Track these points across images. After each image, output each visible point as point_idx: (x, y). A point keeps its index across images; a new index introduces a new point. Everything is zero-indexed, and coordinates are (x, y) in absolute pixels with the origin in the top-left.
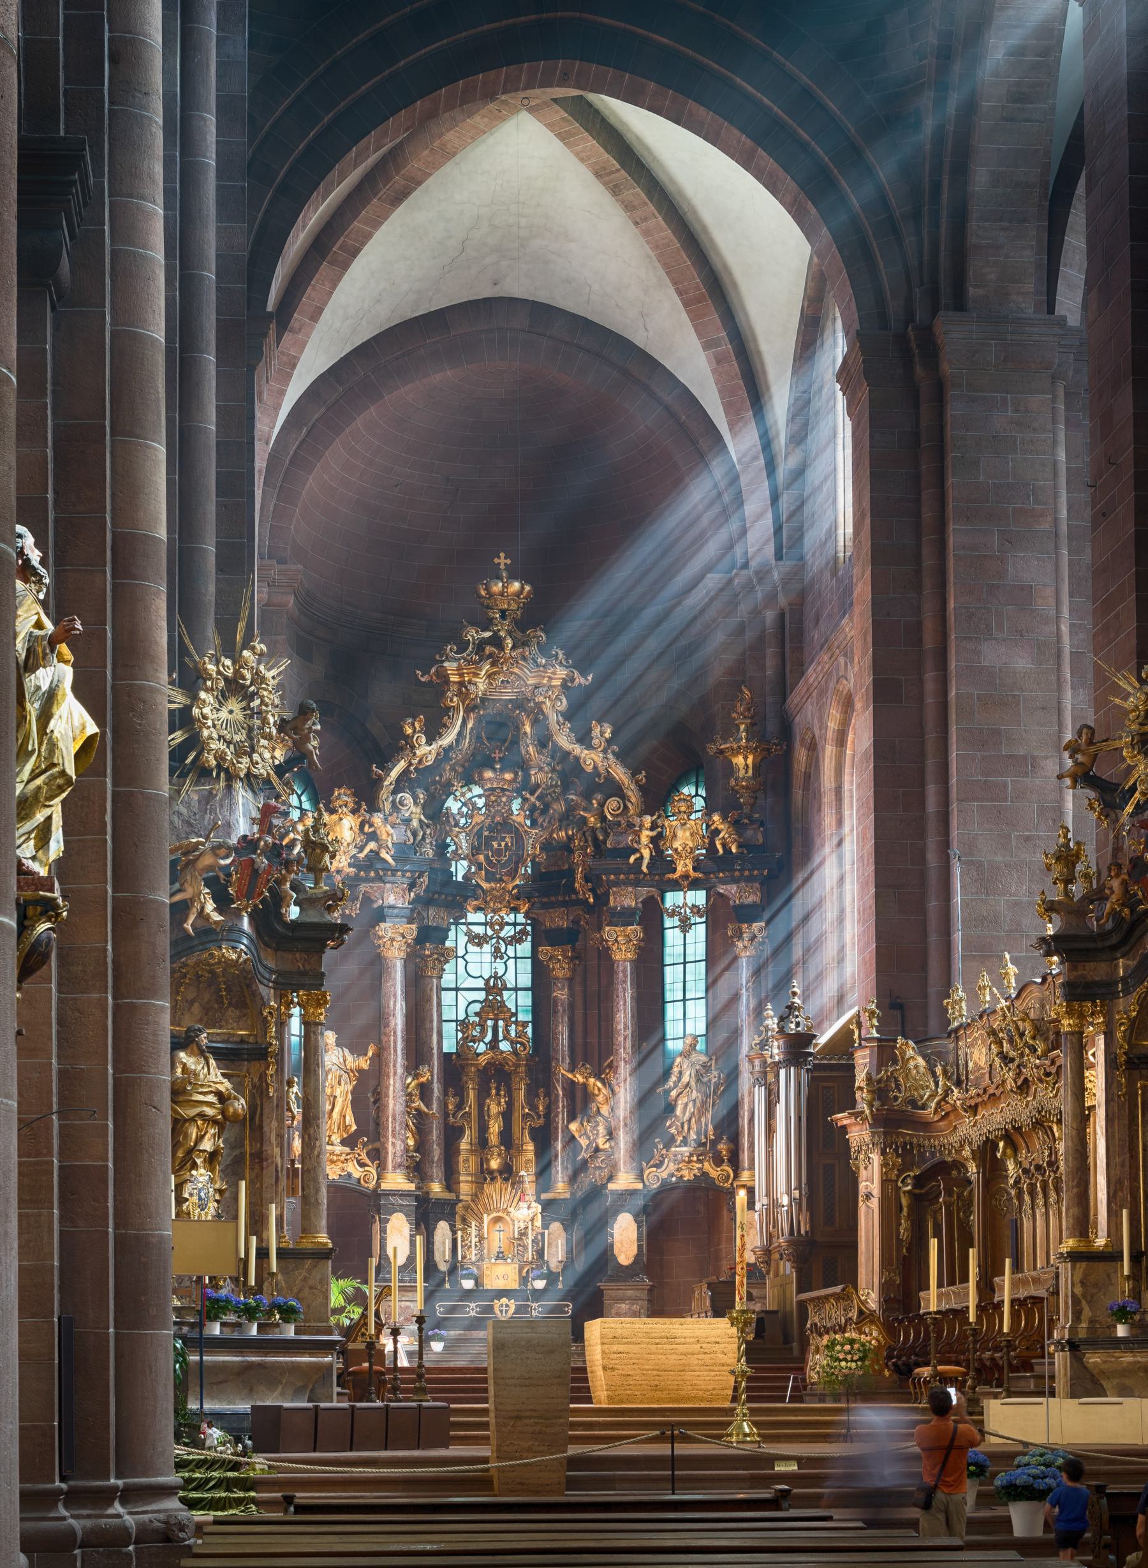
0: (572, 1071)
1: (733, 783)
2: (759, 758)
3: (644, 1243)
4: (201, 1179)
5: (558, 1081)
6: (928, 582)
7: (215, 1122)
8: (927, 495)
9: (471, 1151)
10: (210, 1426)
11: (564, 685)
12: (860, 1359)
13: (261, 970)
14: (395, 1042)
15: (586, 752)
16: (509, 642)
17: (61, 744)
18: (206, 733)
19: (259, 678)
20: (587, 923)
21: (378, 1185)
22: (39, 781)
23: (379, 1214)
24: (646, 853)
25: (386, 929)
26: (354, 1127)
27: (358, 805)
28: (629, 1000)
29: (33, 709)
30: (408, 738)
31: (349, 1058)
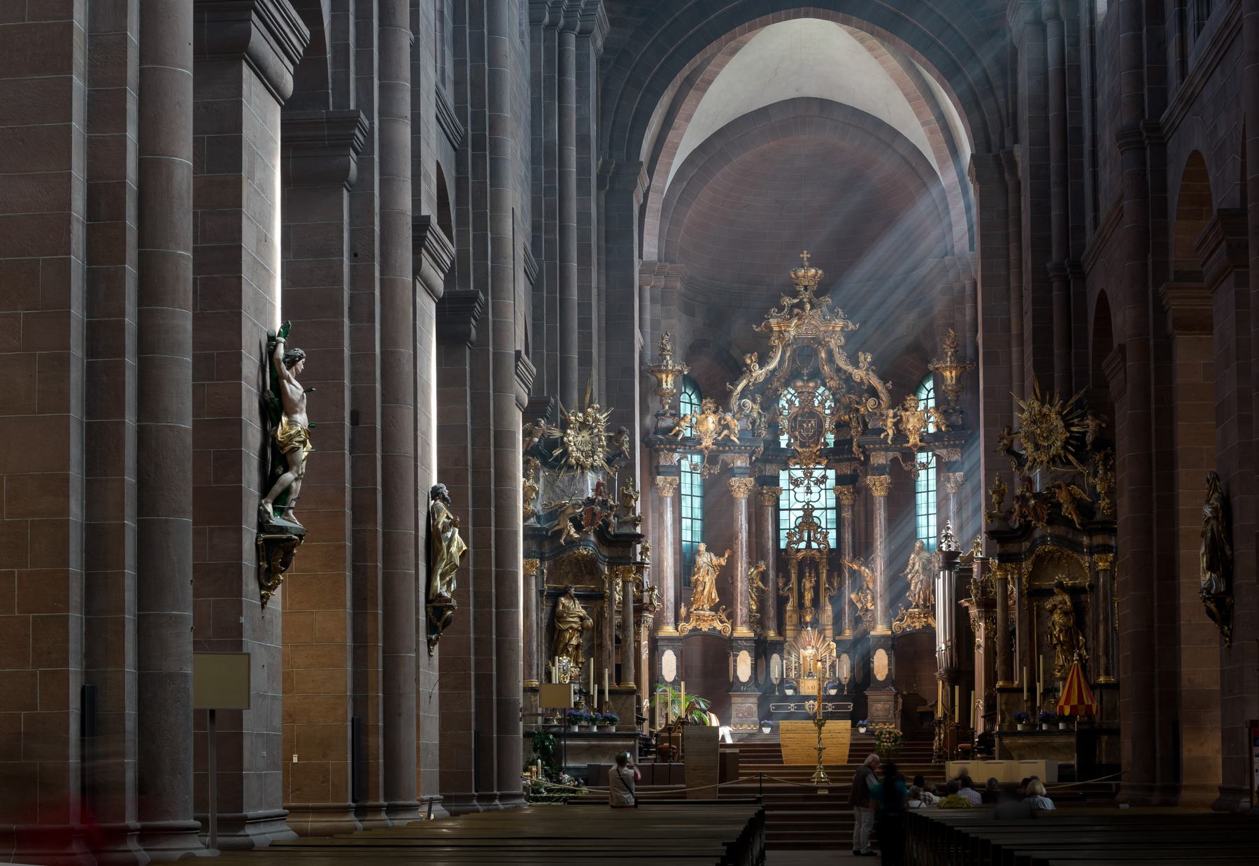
0: (851, 563)
1: (943, 388)
2: (959, 373)
3: (893, 667)
4: (564, 661)
5: (845, 568)
6: (1013, 296)
7: (578, 631)
8: (1013, 246)
9: (793, 611)
10: (564, 774)
11: (842, 328)
12: (893, 741)
13: (601, 557)
14: (742, 549)
15: (856, 371)
16: (808, 306)
17: (454, 555)
18: (570, 448)
19: (596, 420)
20: (861, 472)
21: (732, 633)
22: (447, 567)
23: (733, 651)
24: (891, 432)
26: (718, 600)
27: (717, 408)
28: (883, 520)
29: (445, 544)
30: (747, 366)
31: (714, 559)
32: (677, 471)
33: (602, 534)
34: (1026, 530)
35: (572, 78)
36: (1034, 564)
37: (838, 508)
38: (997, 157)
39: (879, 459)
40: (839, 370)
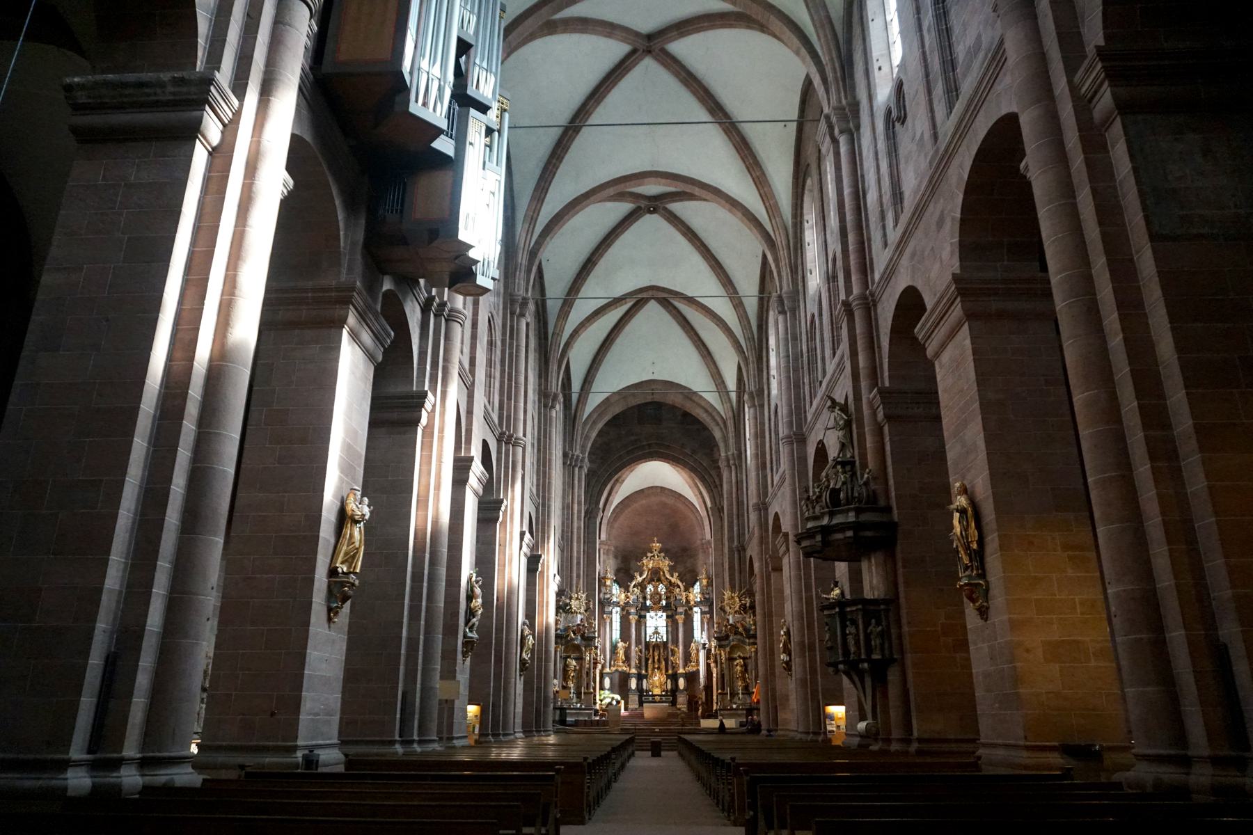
25: (631, 617)
32: (611, 613)
33: (583, 636)
34: (727, 637)
35: (576, 482)
36: (731, 648)
37: (667, 626)
38: (718, 509)
39: (680, 610)
40: (667, 578)
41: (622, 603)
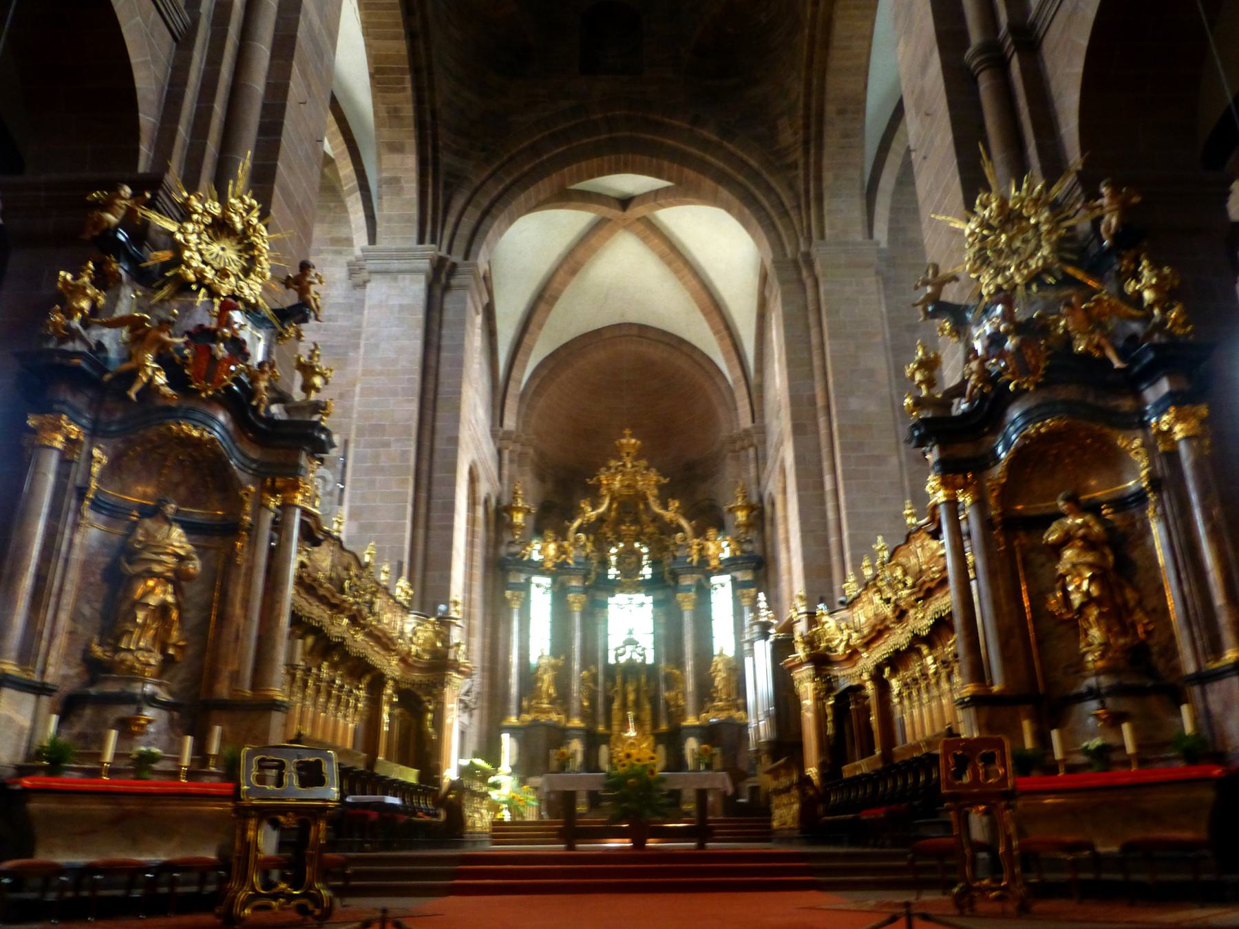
16: (629, 465)
18: (187, 254)
24: (696, 558)
25: (571, 597)
30: (582, 508)
31: (553, 661)
38: (795, 262)
40: (656, 518)
41: (549, 565)
